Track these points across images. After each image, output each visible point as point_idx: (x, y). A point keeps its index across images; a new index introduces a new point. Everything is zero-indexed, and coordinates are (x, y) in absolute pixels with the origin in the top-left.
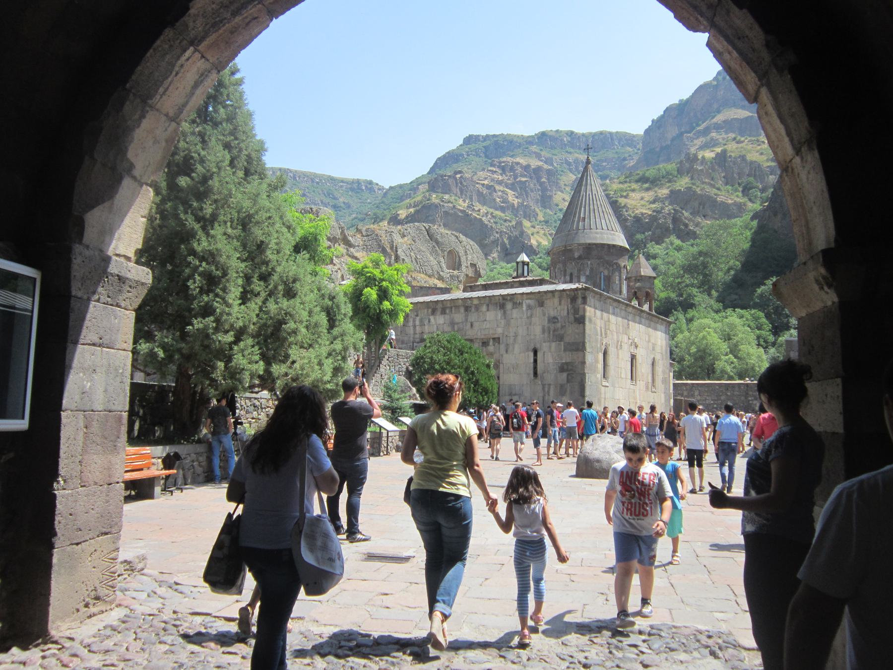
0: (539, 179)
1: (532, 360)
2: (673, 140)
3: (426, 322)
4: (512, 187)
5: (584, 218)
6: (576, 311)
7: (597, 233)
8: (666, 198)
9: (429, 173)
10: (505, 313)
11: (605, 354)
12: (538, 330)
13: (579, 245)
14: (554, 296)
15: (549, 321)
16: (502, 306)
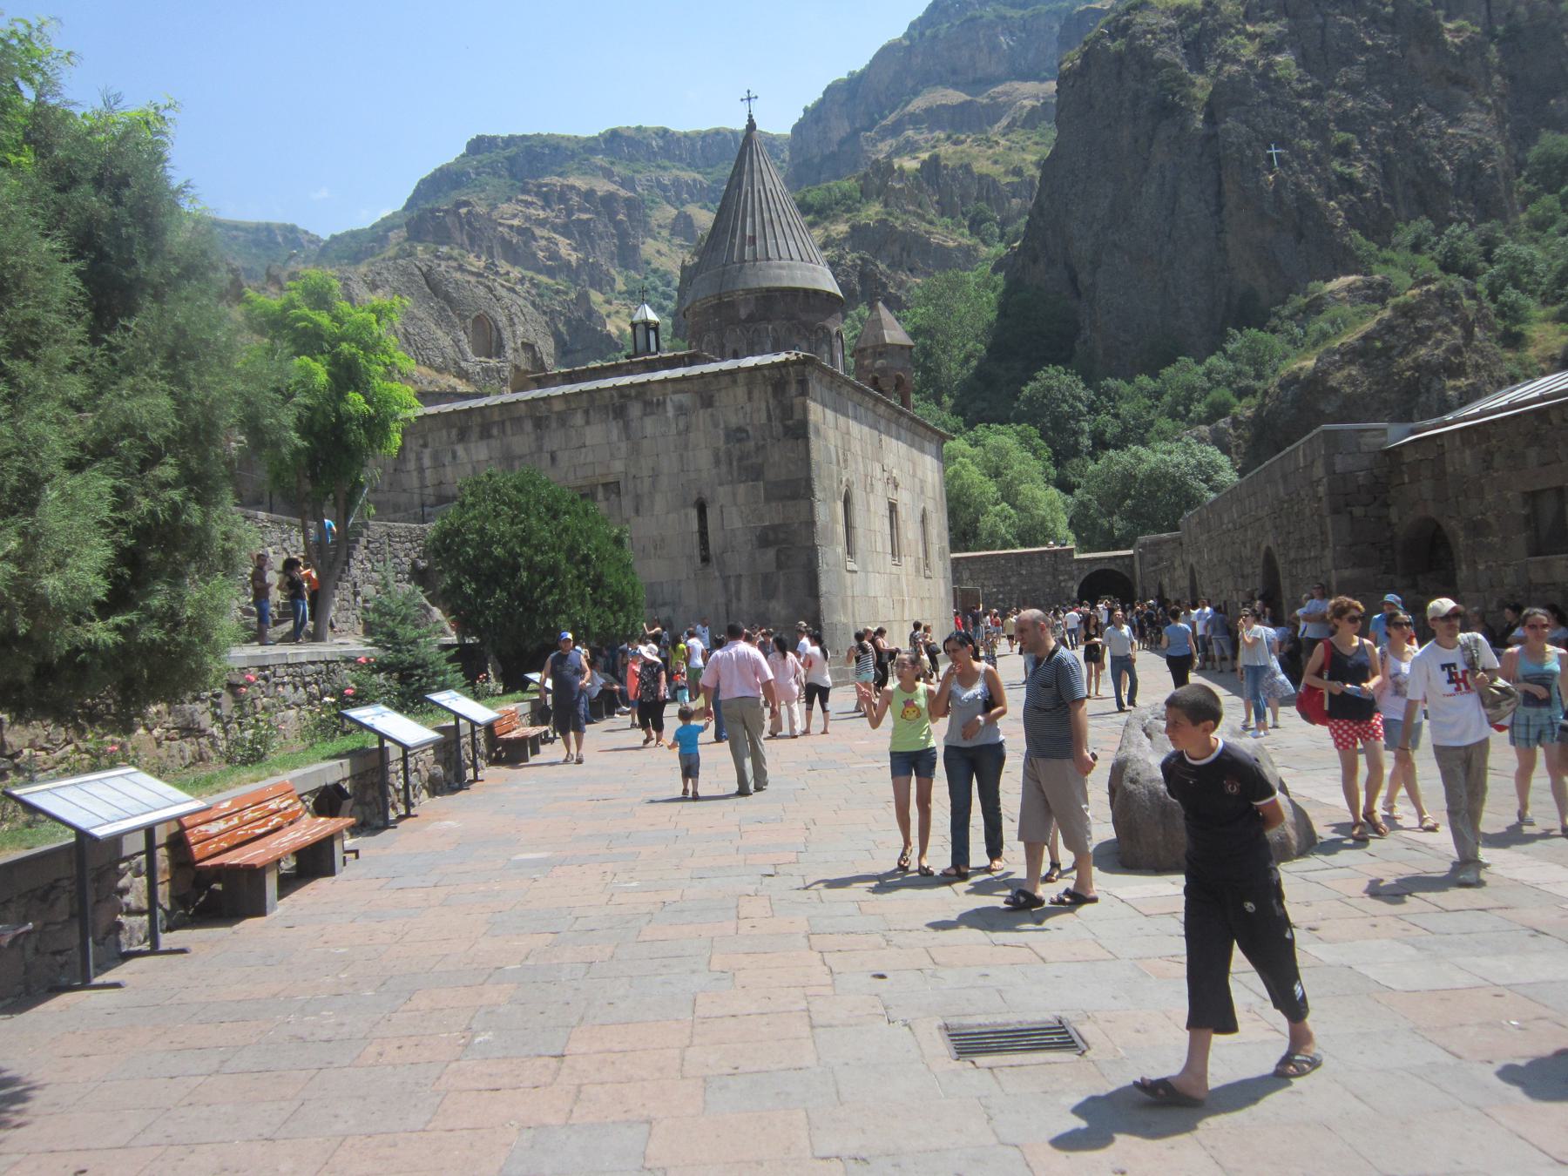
0: (612, 215)
1: (695, 526)
2: (842, 142)
3: (447, 459)
4: (565, 231)
5: (753, 239)
6: (787, 411)
7: (781, 267)
8: (845, 239)
9: (406, 208)
10: (626, 426)
11: (847, 502)
12: (703, 459)
13: (749, 291)
14: (735, 382)
15: (728, 437)
16: (620, 412)
